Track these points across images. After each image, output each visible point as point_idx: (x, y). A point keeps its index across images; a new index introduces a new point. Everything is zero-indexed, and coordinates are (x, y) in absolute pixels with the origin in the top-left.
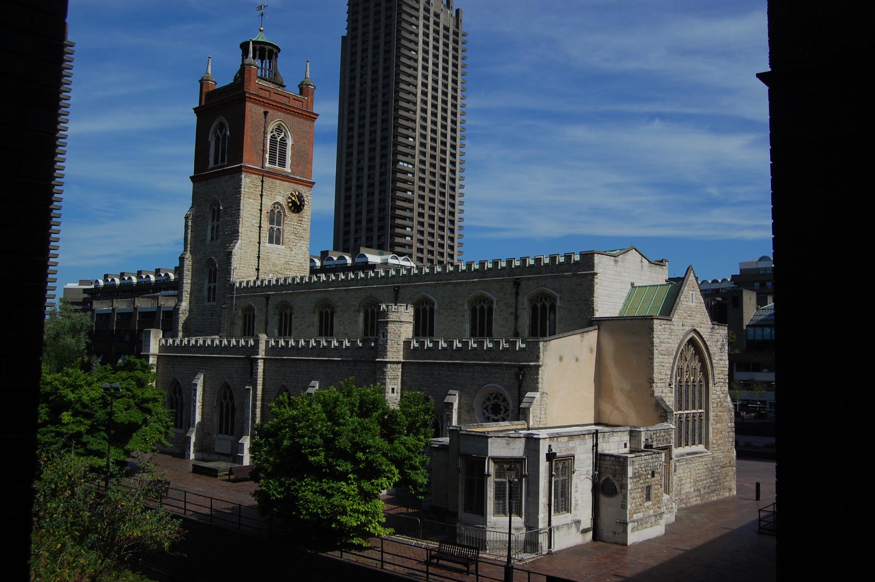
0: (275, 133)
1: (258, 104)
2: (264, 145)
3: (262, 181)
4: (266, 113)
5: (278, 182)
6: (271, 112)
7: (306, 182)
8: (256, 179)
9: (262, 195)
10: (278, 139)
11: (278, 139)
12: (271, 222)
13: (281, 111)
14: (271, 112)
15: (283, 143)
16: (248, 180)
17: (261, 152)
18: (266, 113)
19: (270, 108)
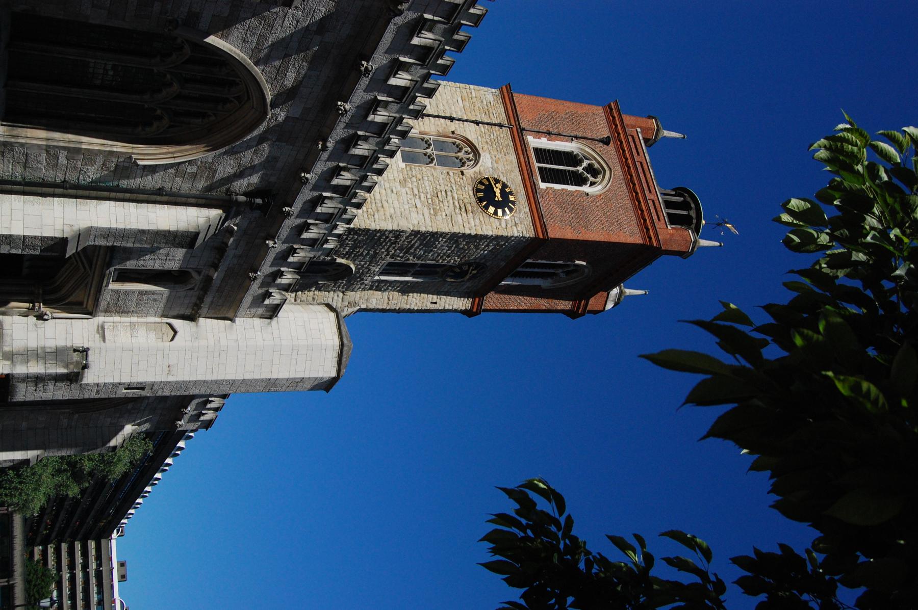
0: (585, 164)
1: (610, 127)
2: (559, 135)
3: (500, 125)
4: (606, 141)
5: (513, 157)
6: (611, 149)
7: (541, 217)
8: (499, 114)
9: (477, 123)
10: (580, 169)
11: (580, 169)
12: (440, 146)
13: (624, 173)
14: (611, 149)
15: (579, 180)
16: (490, 97)
17: (544, 129)
18: (606, 141)
19: (617, 150)
